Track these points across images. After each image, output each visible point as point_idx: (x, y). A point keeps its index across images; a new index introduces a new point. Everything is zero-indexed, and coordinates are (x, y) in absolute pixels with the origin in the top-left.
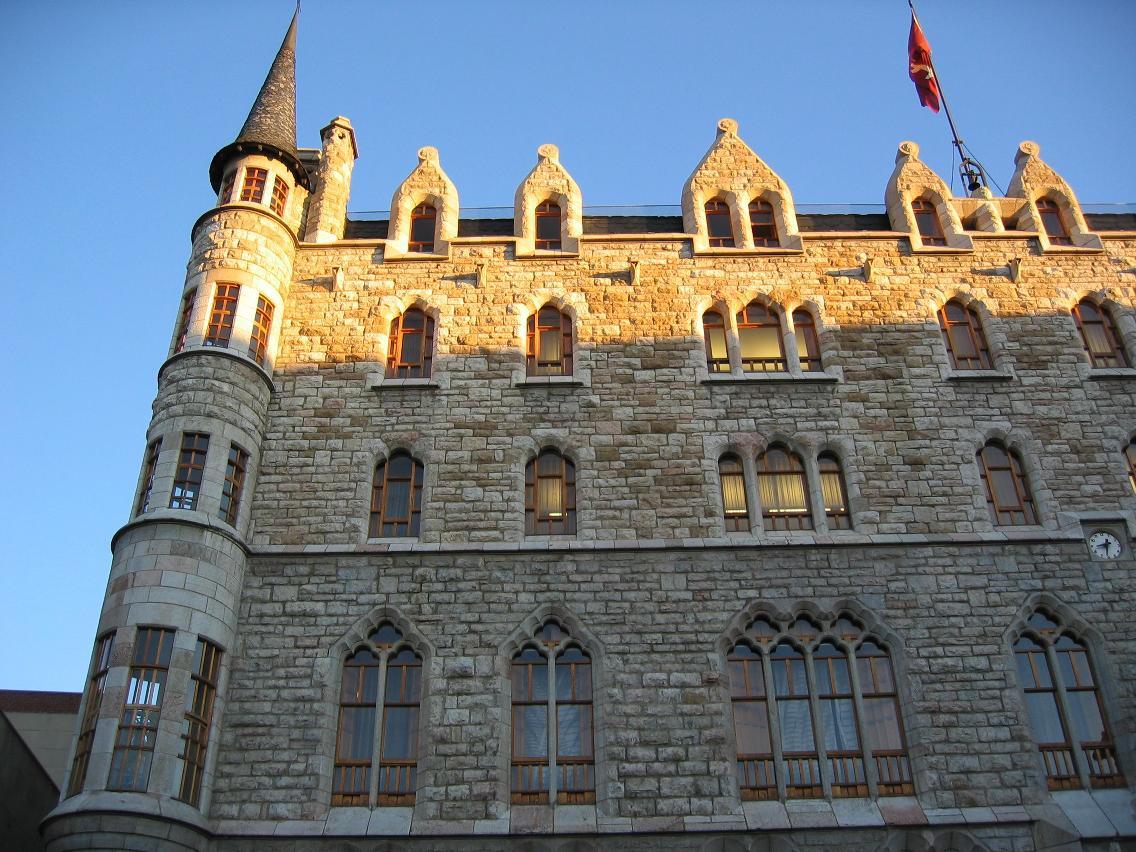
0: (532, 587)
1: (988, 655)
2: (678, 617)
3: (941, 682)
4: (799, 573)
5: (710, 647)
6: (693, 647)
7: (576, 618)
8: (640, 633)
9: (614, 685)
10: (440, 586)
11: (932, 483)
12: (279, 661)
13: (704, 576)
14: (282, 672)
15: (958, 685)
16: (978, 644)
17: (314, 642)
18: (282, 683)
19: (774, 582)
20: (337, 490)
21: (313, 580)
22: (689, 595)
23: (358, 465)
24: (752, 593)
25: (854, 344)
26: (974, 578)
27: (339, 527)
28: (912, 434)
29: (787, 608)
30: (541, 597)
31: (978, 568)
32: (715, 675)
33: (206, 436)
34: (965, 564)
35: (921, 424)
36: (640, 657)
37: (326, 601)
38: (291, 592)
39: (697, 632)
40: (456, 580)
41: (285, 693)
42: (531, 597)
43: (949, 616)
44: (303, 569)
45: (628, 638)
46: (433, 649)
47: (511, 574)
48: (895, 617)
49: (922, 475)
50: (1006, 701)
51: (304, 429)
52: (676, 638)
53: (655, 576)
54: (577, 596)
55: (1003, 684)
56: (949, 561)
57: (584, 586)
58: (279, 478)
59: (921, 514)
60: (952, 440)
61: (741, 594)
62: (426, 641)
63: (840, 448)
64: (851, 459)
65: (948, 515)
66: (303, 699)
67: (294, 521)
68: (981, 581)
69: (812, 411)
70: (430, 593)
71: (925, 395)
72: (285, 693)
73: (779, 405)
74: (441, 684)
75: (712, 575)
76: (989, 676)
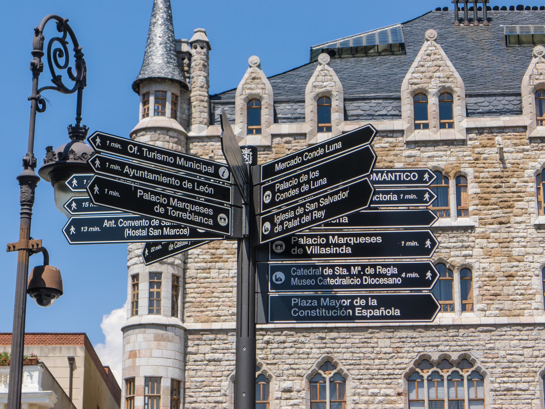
0: (318, 346)
1: (528, 382)
2: (385, 361)
3: (505, 395)
4: (443, 338)
5: (399, 376)
6: (391, 377)
7: (338, 361)
8: (368, 369)
9: (354, 395)
10: (275, 345)
11: (516, 287)
12: (204, 383)
13: (399, 340)
14: (207, 389)
15: (512, 397)
16: (524, 377)
17: (219, 374)
18: (208, 394)
19: (431, 343)
20: (224, 292)
21: (217, 342)
22: (390, 350)
23: (233, 277)
24: (421, 349)
25: (487, 202)
26: (528, 342)
27: (225, 312)
28: (510, 257)
29: (435, 357)
30: (323, 351)
31: (530, 337)
32: (401, 390)
33: (161, 273)
34: (525, 333)
35: (515, 252)
36: (368, 381)
37: (224, 353)
38: (207, 349)
39: (394, 369)
40: (284, 342)
41: (209, 399)
42: (318, 351)
43: (512, 362)
44: (212, 336)
45: (362, 372)
46: (274, 377)
47: (308, 339)
48: (487, 362)
49: (514, 282)
50: (533, 405)
51: (204, 256)
52: (384, 372)
53: (376, 340)
54: (339, 350)
55: (533, 397)
56: (517, 333)
57: (342, 345)
58: (194, 285)
59: (507, 305)
60: (531, 262)
61: (416, 349)
62: (271, 374)
63: (472, 267)
64: (476, 274)
65: (522, 306)
66: (215, 402)
67: (204, 309)
68: (530, 344)
69: (460, 244)
70: (271, 349)
71: (521, 234)
72: (209, 399)
73: (443, 241)
74: (279, 394)
75: (402, 340)
76: (526, 392)
